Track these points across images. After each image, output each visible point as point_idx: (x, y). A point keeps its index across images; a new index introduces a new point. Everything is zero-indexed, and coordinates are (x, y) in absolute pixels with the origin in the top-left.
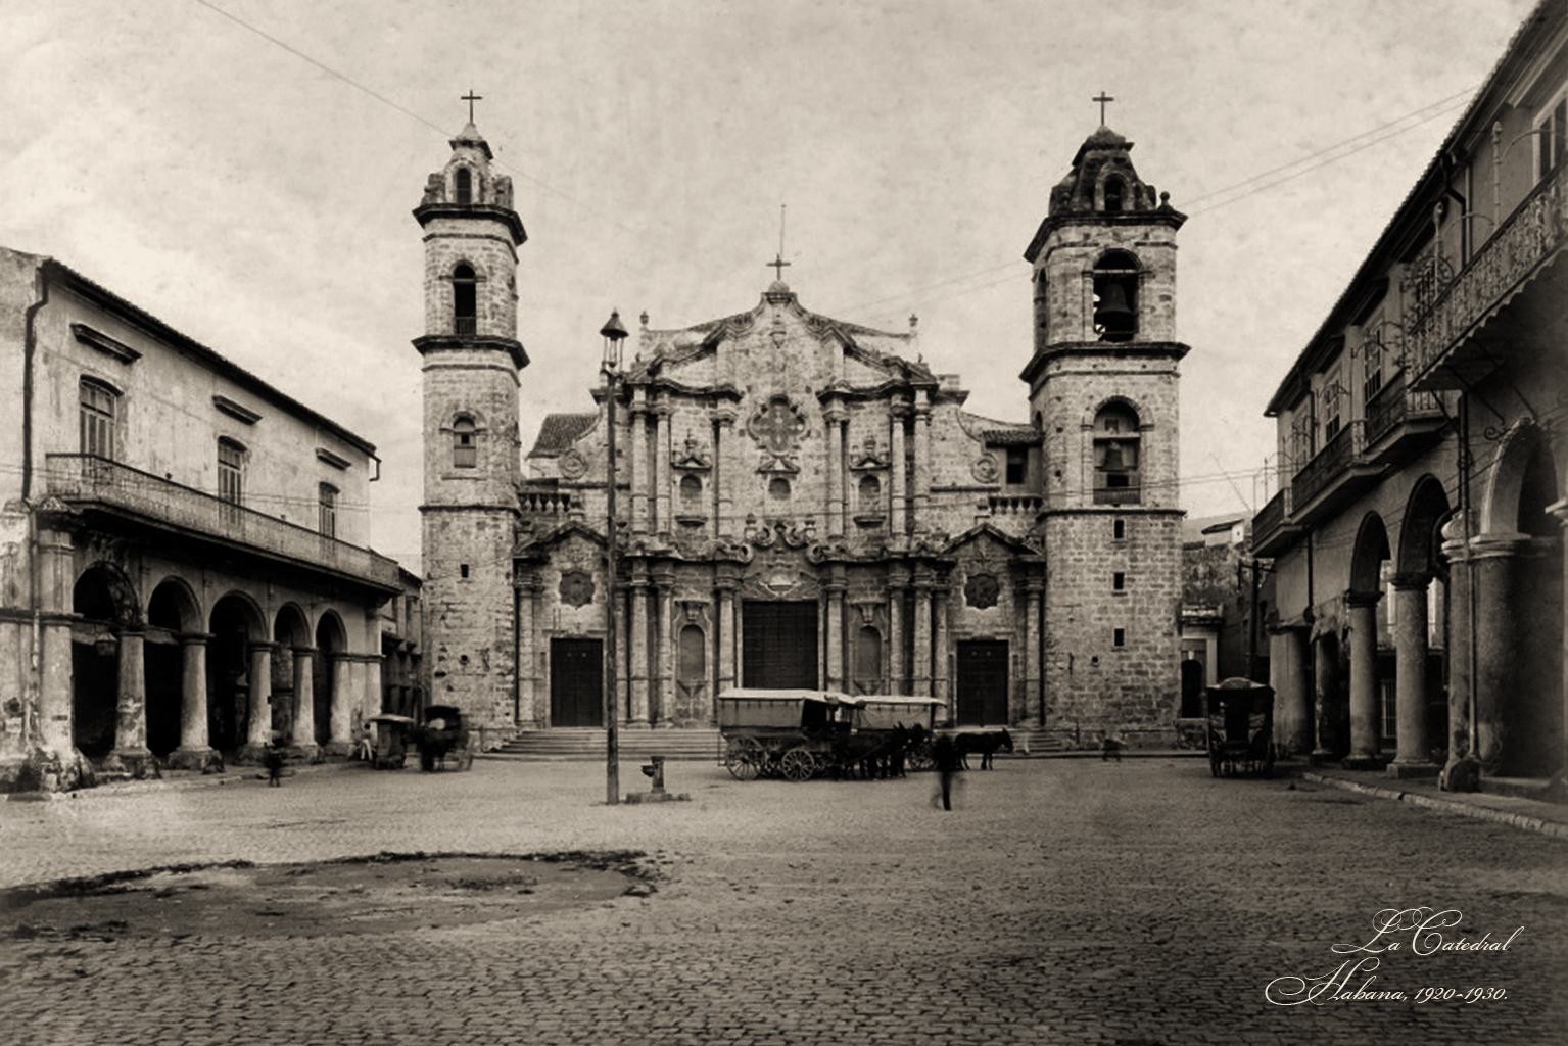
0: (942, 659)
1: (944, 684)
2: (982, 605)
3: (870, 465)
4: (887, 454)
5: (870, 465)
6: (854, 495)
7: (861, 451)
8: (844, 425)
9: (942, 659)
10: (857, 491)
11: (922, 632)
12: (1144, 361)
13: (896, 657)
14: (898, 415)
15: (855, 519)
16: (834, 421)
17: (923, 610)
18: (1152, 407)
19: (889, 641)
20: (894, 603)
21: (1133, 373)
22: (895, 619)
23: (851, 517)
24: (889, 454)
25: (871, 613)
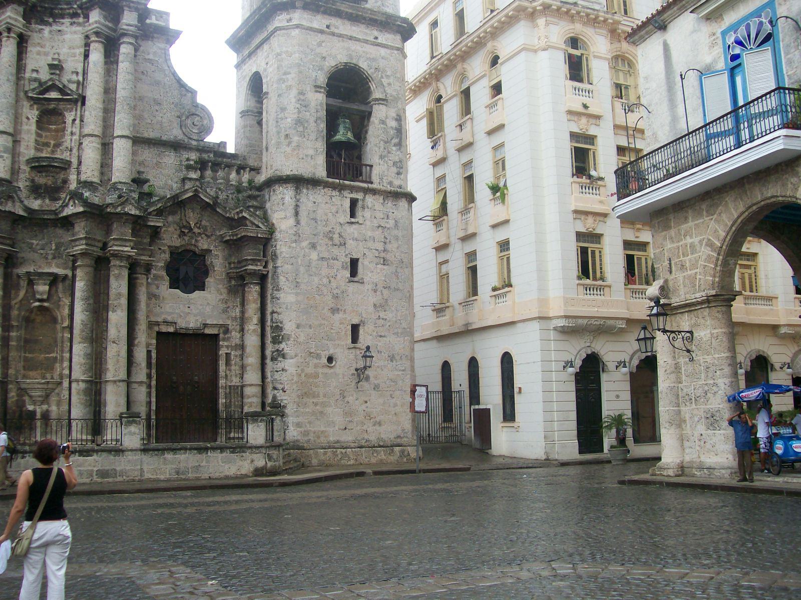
0: (140, 355)
1: (143, 389)
2: (188, 290)
3: (54, 95)
4: (78, 83)
5: (54, 95)
6: (29, 128)
7: (44, 75)
8: (22, 42)
9: (140, 355)
10: (33, 127)
11: (117, 319)
12: (376, 33)
13: (80, 349)
14: (97, 34)
15: (28, 162)
16: (9, 30)
17: (118, 286)
18: (385, 81)
19: (71, 328)
20: (79, 273)
21: (366, 42)
22: (78, 294)
23: (23, 159)
24: (82, 84)
25: (47, 288)
